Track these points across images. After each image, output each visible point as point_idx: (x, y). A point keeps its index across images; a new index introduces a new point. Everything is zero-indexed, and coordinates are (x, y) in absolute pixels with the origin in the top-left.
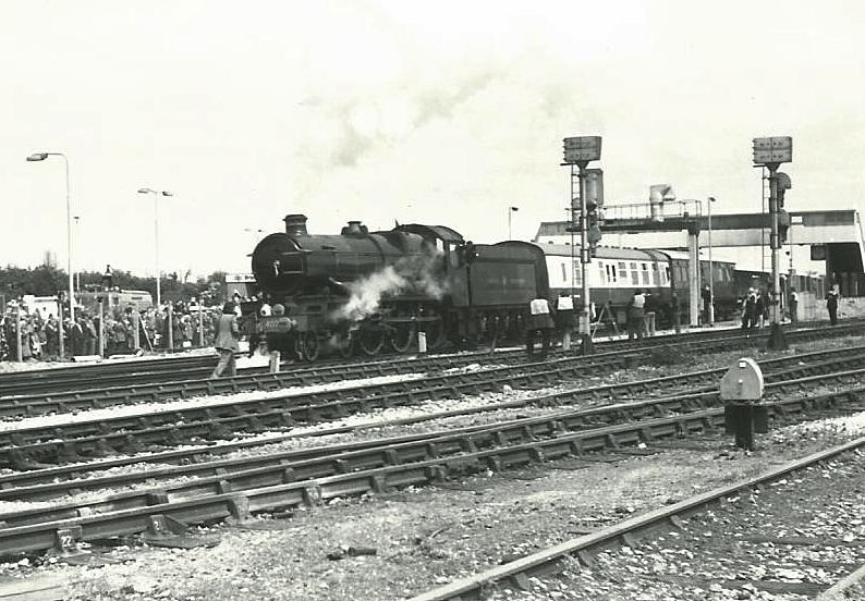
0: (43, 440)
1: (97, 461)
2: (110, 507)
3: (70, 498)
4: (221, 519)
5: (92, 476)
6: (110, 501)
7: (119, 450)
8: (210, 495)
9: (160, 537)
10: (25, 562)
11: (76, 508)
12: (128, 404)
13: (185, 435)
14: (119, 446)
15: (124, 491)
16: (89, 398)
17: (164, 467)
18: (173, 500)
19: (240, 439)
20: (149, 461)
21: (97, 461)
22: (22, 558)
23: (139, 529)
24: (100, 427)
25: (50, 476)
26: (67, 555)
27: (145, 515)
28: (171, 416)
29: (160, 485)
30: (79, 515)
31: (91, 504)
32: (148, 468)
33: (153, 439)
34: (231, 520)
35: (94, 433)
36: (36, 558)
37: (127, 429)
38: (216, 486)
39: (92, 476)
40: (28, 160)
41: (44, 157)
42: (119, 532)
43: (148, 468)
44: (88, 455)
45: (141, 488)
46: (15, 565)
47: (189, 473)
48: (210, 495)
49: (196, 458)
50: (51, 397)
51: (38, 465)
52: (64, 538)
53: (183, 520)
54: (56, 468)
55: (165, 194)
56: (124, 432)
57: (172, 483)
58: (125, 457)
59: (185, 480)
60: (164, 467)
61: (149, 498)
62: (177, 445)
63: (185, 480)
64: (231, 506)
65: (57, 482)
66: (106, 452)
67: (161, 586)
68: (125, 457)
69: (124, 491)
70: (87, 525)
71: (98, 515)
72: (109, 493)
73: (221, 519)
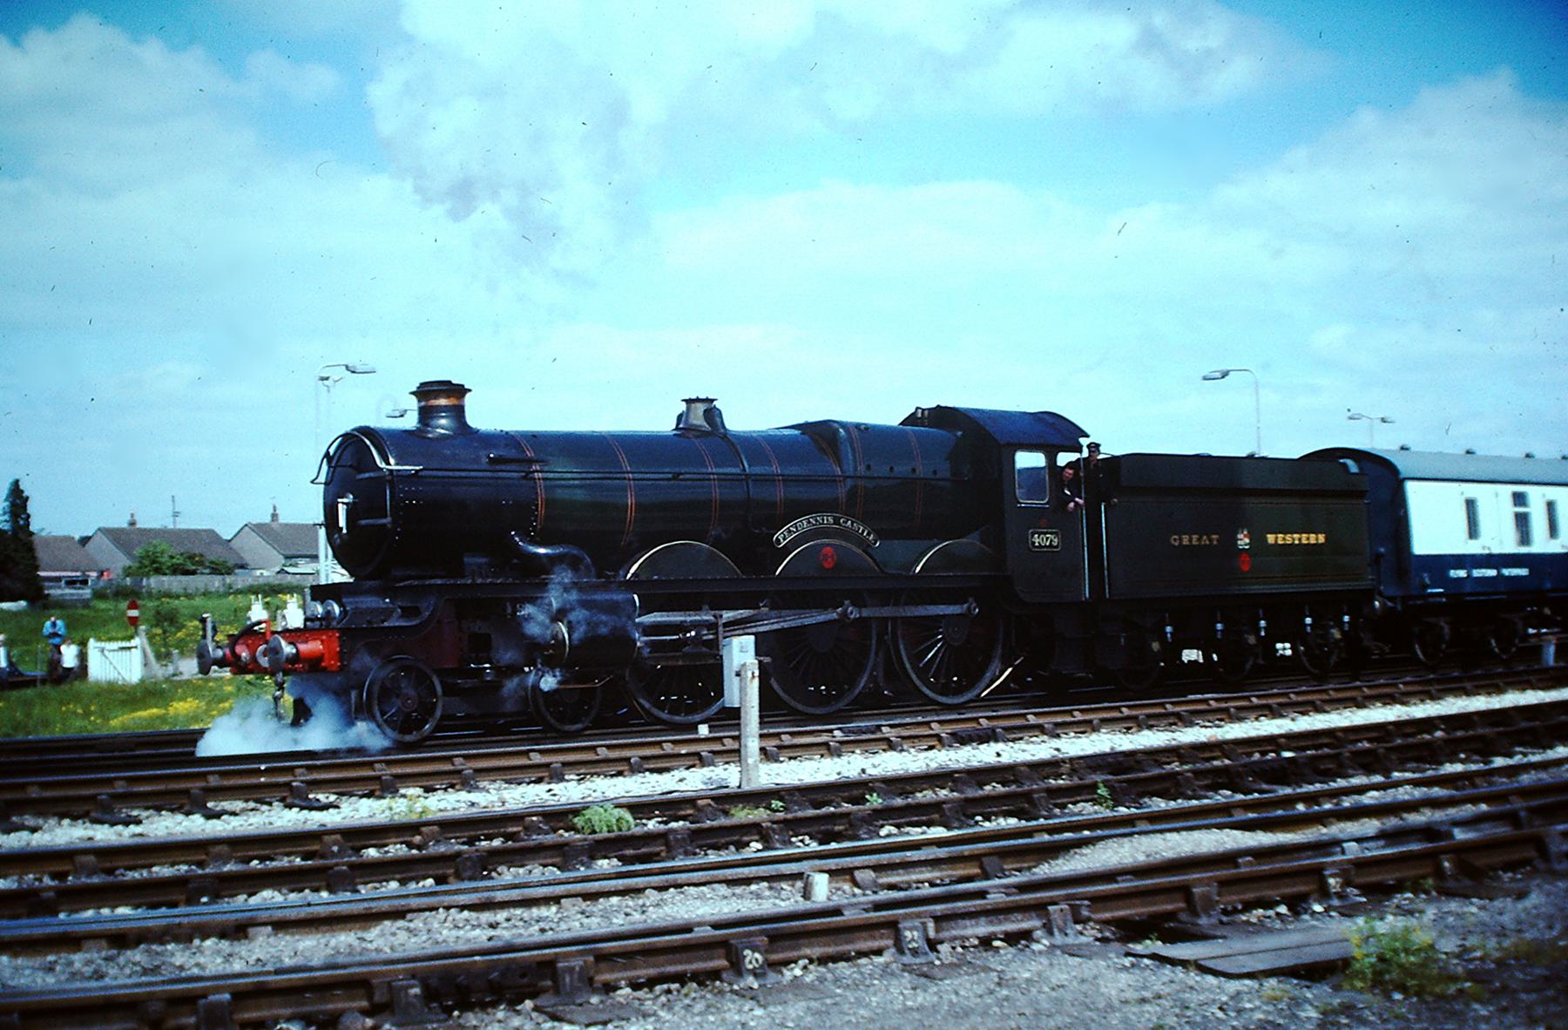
0: (1263, 753)
1: (1341, 783)
2: (1382, 843)
3: (1324, 830)
4: (1528, 862)
5: (1347, 803)
6: (1382, 835)
7: (1369, 771)
8: (1502, 830)
9: (1451, 884)
10: (1283, 909)
11: (1337, 843)
12: (1361, 706)
13: (1449, 751)
14: (1368, 763)
15: (1392, 822)
16: (1309, 698)
17: (1437, 791)
18: (1460, 835)
19: (1525, 755)
20: (1416, 783)
21: (1341, 783)
22: (1278, 903)
23: (1421, 872)
24: (1336, 737)
25: (1290, 801)
26: (1336, 902)
27: (1432, 857)
28: (1428, 724)
29: (1438, 815)
30: (1343, 852)
31: (1355, 837)
32: (1418, 793)
33: (1410, 755)
34: (1542, 866)
35: (1327, 745)
36: (1297, 905)
37: (1370, 740)
38: (1511, 818)
39: (1347, 803)
40: (1205, 379)
41: (1225, 374)
42: (1397, 875)
43: (1418, 793)
44: (1333, 775)
45: (1414, 818)
46: (1271, 913)
47: (1474, 800)
48: (1502, 830)
49: (1478, 781)
50: (1216, 700)
51: (1265, 786)
52: (1332, 881)
53: (1481, 861)
54: (1288, 791)
55: (1383, 420)
56: (1367, 745)
57: (1452, 812)
58: (1378, 779)
59: (1469, 810)
60: (1437, 791)
61: (1428, 832)
62: (1441, 764)
63: (1469, 810)
64: (1539, 844)
65: (1301, 807)
66: (1351, 772)
67: (1467, 944)
68: (1378, 779)
69: (1392, 822)
70: (1361, 864)
71: (1369, 854)
72: (1371, 826)
73: (1528, 862)
